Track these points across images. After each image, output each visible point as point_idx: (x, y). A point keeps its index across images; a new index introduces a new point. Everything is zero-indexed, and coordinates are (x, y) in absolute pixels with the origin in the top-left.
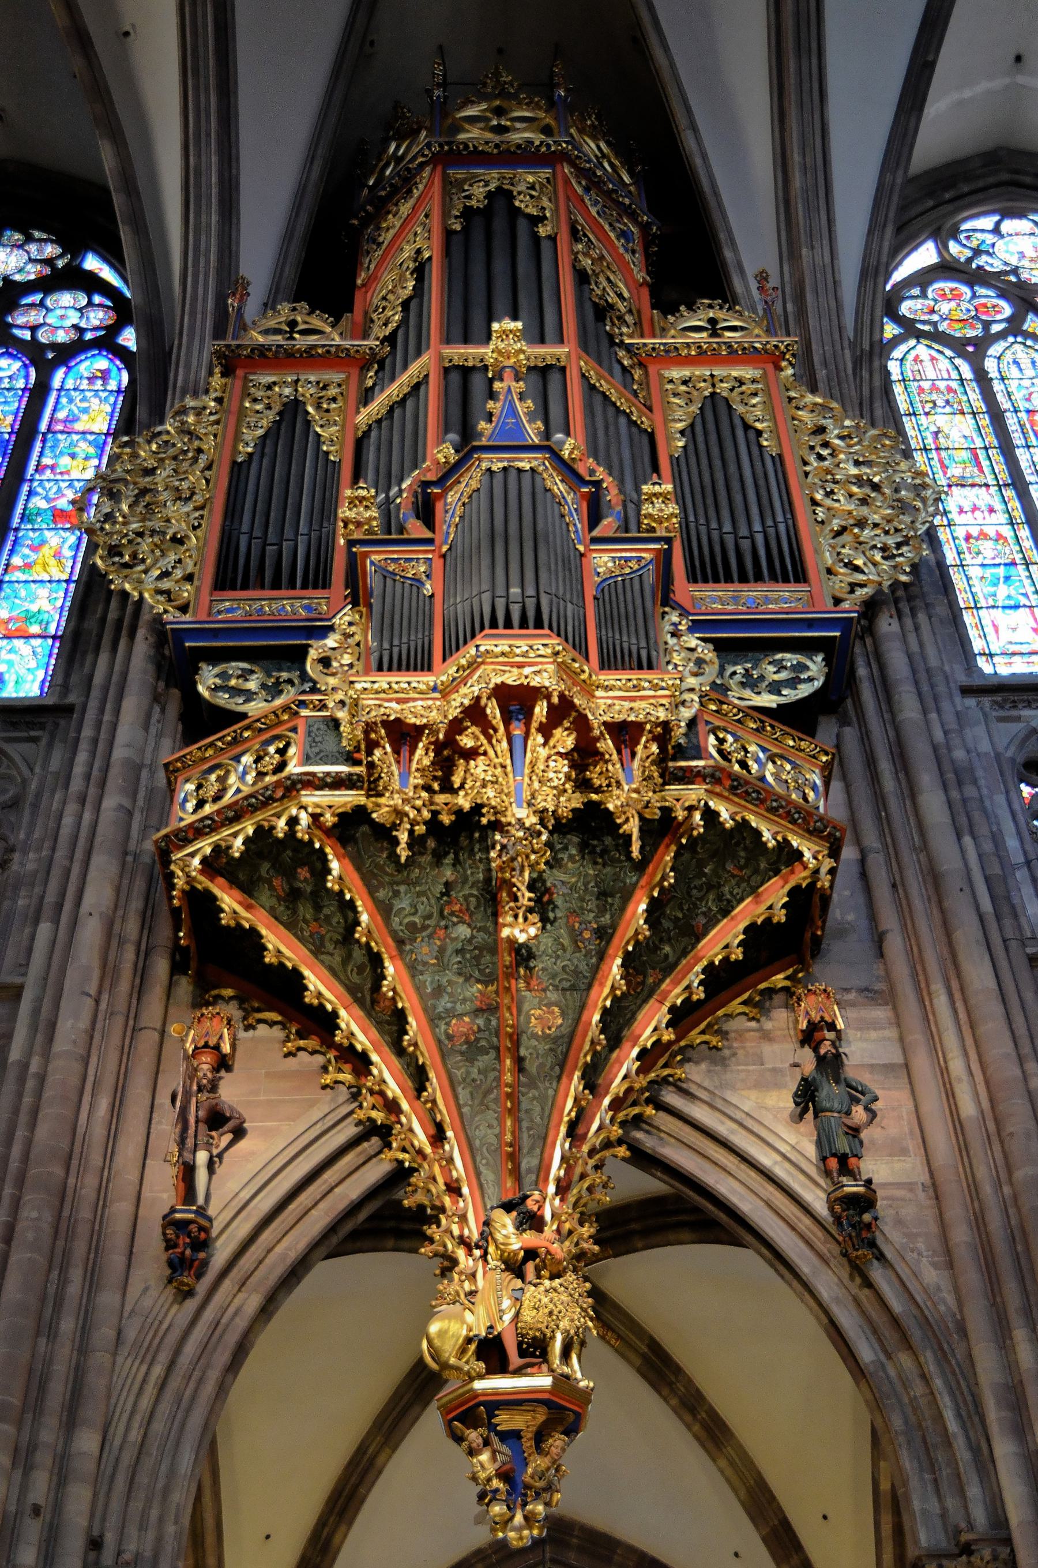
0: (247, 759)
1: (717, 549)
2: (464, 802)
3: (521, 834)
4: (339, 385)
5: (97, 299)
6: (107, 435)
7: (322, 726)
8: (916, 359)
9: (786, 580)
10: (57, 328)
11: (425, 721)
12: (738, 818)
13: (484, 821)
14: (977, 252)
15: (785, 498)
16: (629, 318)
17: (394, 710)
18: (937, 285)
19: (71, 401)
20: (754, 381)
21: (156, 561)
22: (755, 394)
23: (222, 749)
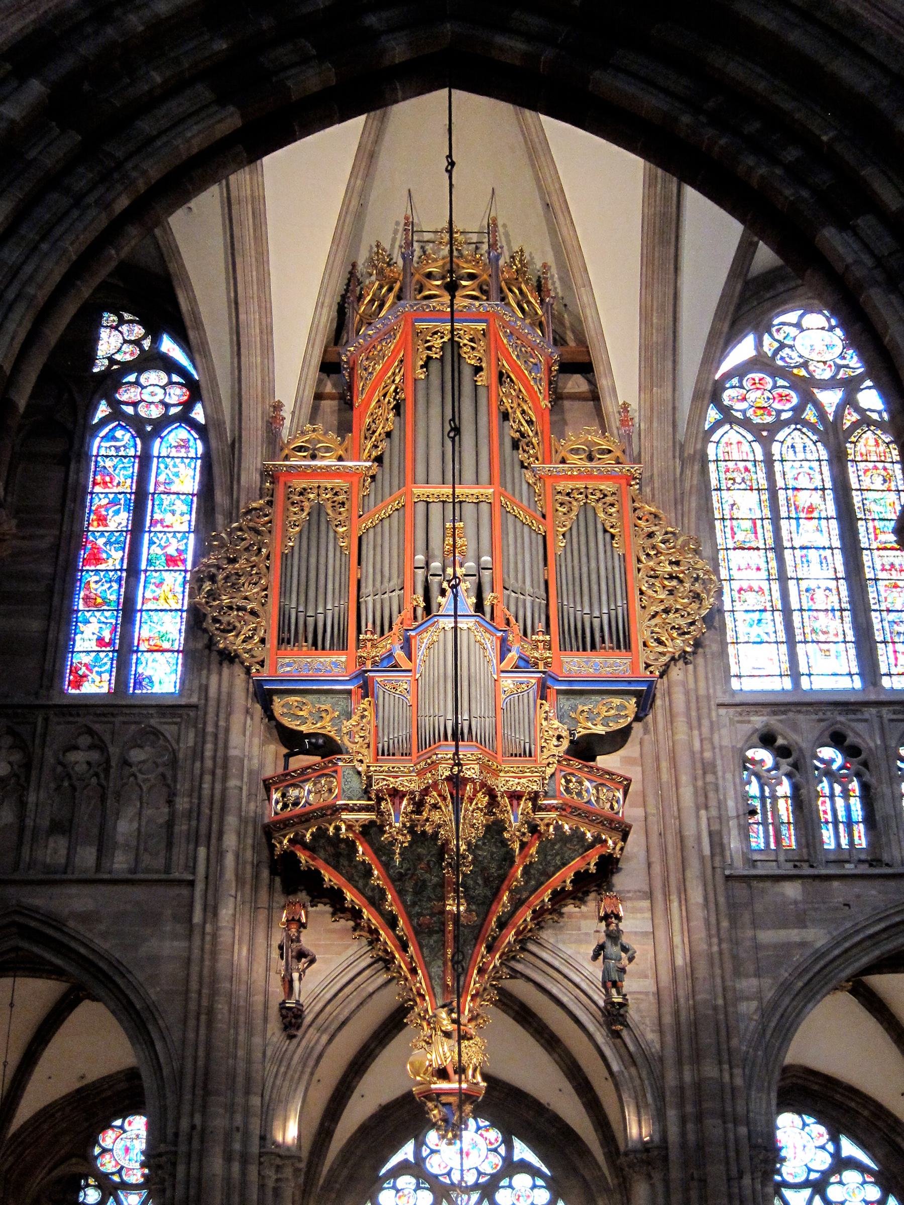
5: (175, 378)
14: (782, 346)
16: (535, 441)
18: (750, 376)
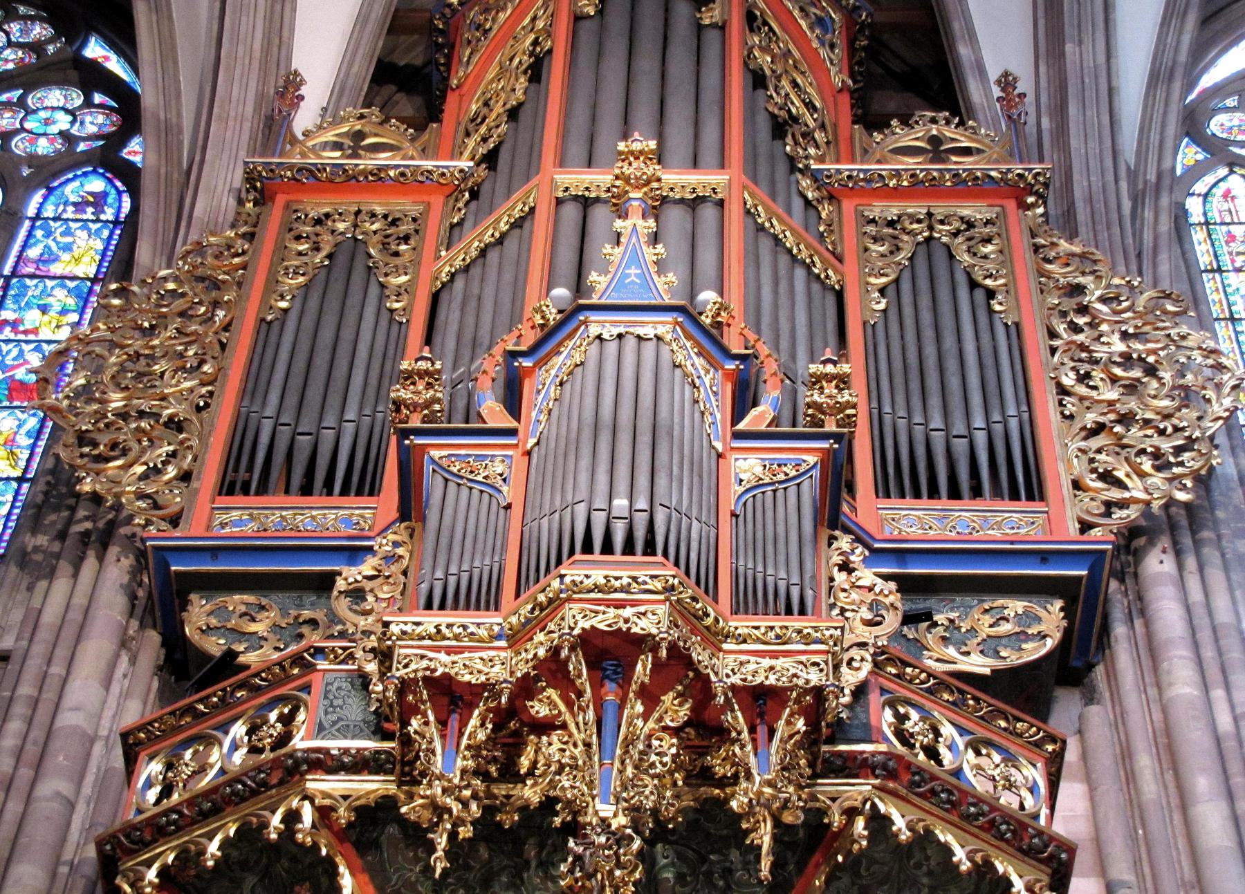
0: (239, 730)
1: (921, 451)
2: (531, 793)
3: (603, 839)
4: (414, 220)
5: (98, 98)
6: (94, 280)
7: (344, 685)
8: (1227, 194)
9: (1015, 496)
10: (39, 135)
11: (483, 678)
12: (920, 827)
13: (557, 821)
15: (1020, 382)
16: (819, 136)
17: (442, 663)
19: (48, 234)
20: (988, 222)
21: (143, 451)
22: (988, 241)
23: (204, 714)
